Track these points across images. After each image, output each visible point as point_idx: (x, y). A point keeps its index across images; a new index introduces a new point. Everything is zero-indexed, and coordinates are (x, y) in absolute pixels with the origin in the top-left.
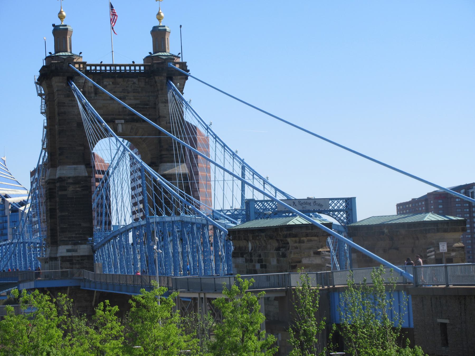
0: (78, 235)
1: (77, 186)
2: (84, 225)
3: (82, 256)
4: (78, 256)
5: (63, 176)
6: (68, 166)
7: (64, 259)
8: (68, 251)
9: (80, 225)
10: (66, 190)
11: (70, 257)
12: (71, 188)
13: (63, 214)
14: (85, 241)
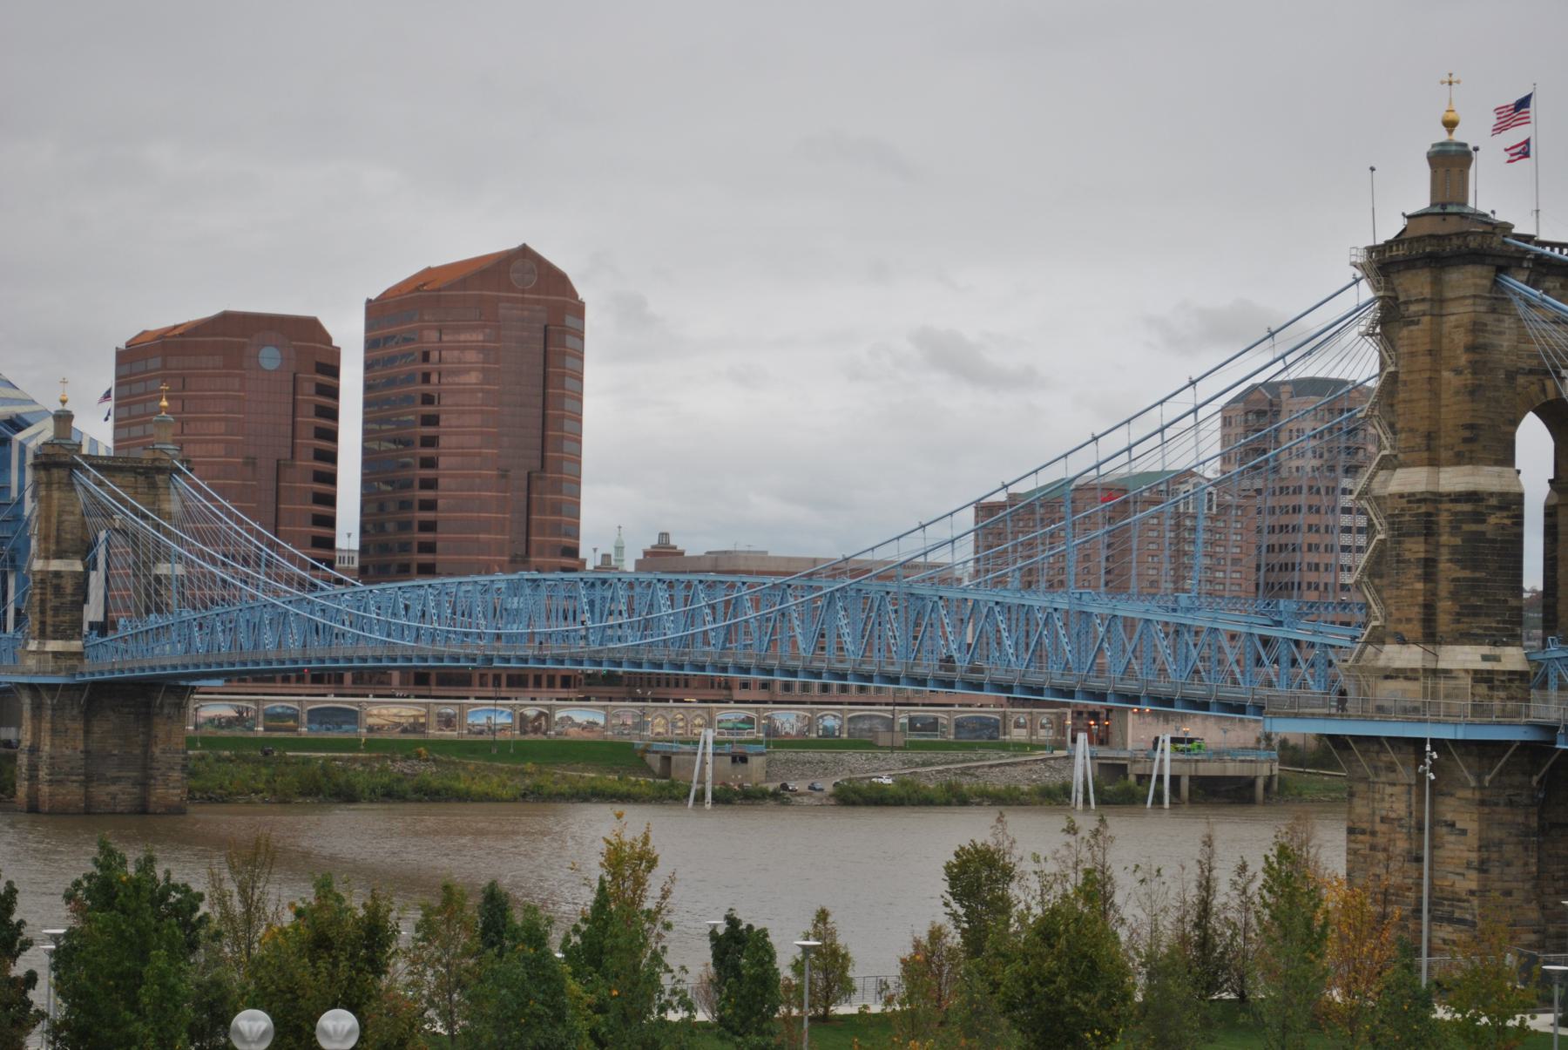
1: (1505, 514)
4: (1504, 672)
5: (1480, 488)
6: (1487, 468)
7: (1480, 677)
8: (1485, 658)
10: (1484, 521)
11: (1488, 672)
12: (1493, 520)
13: (1477, 575)
14: (1514, 639)
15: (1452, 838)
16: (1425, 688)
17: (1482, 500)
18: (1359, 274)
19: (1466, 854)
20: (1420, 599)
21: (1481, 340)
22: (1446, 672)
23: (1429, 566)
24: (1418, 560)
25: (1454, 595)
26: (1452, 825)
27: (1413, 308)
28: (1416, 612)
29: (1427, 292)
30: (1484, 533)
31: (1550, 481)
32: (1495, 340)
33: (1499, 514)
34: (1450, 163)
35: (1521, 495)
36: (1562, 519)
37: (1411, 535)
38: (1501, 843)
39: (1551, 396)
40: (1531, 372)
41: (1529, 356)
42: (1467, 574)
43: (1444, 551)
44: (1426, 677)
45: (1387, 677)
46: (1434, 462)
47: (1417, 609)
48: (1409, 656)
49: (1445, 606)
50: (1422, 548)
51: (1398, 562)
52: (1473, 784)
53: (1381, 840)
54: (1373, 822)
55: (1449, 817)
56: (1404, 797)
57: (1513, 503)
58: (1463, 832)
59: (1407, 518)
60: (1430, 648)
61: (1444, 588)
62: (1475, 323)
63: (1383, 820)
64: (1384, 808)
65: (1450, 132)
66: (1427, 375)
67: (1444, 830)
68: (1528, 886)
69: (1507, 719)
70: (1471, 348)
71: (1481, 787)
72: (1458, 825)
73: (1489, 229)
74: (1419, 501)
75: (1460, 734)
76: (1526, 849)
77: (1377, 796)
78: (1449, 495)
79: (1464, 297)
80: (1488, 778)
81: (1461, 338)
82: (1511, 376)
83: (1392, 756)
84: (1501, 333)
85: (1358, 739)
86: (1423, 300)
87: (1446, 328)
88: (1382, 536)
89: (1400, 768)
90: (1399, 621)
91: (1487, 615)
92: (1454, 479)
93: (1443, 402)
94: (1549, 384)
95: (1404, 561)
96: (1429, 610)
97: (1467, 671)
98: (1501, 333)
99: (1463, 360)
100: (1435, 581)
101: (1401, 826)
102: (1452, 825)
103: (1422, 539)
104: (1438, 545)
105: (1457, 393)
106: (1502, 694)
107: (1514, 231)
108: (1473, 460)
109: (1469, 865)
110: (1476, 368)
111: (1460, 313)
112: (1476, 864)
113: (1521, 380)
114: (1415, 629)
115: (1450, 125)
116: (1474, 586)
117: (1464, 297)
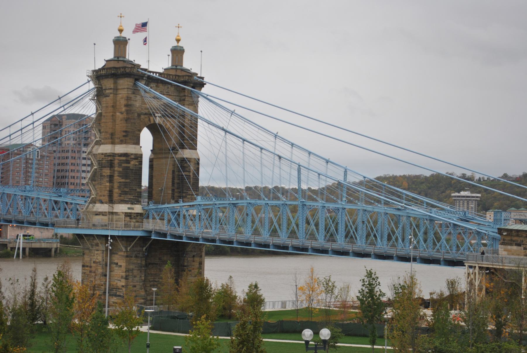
3: (137, 213)
4: (135, 213)
5: (128, 152)
7: (127, 215)
8: (129, 208)
10: (129, 163)
11: (130, 213)
12: (132, 163)
13: (127, 181)
14: (138, 202)
15: (117, 268)
16: (109, 218)
17: (129, 156)
18: (90, 79)
19: (121, 274)
20: (108, 189)
21: (130, 103)
22: (116, 213)
23: (111, 178)
24: (108, 175)
25: (119, 187)
26: (117, 264)
27: (107, 91)
28: (106, 193)
29: (112, 86)
30: (129, 167)
31: (151, 151)
32: (134, 103)
33: (134, 161)
34: (121, 43)
35: (142, 155)
36: (155, 163)
37: (105, 167)
38: (133, 270)
39: (152, 122)
40: (146, 114)
41: (145, 109)
42: (123, 180)
43: (116, 173)
44: (109, 215)
45: (96, 215)
46: (113, 143)
47: (107, 192)
48: (104, 208)
49: (116, 191)
50: (109, 171)
51: (101, 176)
52: (124, 250)
53: (93, 269)
54: (91, 263)
55: (116, 261)
56: (101, 255)
57: (139, 157)
58: (121, 266)
59: (104, 161)
60: (111, 205)
61: (116, 185)
62: (128, 97)
63: (94, 262)
64: (94, 258)
65: (121, 33)
66: (112, 114)
67: (114, 265)
68: (141, 284)
69: (135, 228)
70: (126, 106)
71: (127, 251)
72: (119, 264)
73: (133, 66)
74: (108, 156)
75: (120, 234)
76: (141, 272)
77: (92, 254)
78: (118, 154)
79: (124, 88)
80: (129, 248)
81: (123, 102)
82: (139, 115)
83: (97, 241)
84: (136, 101)
85: (86, 235)
86: (111, 89)
87: (118, 99)
88: (96, 167)
89: (100, 245)
90: (101, 196)
91: (130, 194)
92: (120, 149)
93: (117, 123)
94: (151, 118)
95: (103, 176)
96: (111, 192)
97: (123, 213)
98: (136, 101)
99: (124, 109)
100: (113, 183)
101: (100, 264)
102: (117, 264)
103: (109, 168)
104: (114, 171)
105: (121, 120)
106: (134, 220)
107: (141, 67)
108: (126, 143)
109: (122, 277)
110: (128, 112)
111: (123, 93)
112: (124, 277)
113: (142, 117)
114: (106, 198)
115: (121, 31)
116: (126, 184)
117: (124, 88)
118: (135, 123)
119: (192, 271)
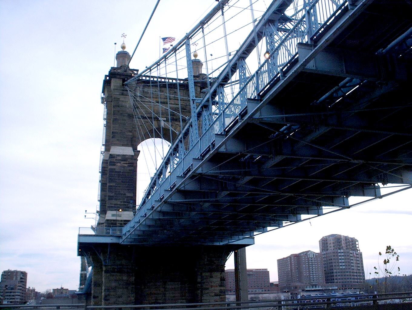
0: (122, 203)
1: (125, 162)
2: (128, 195)
4: (122, 221)
8: (113, 215)
9: (125, 194)
11: (114, 220)
13: (111, 184)
17: (114, 157)
30: (115, 169)
33: (122, 162)
91: (116, 199)
118: (124, 124)
119: (210, 289)
